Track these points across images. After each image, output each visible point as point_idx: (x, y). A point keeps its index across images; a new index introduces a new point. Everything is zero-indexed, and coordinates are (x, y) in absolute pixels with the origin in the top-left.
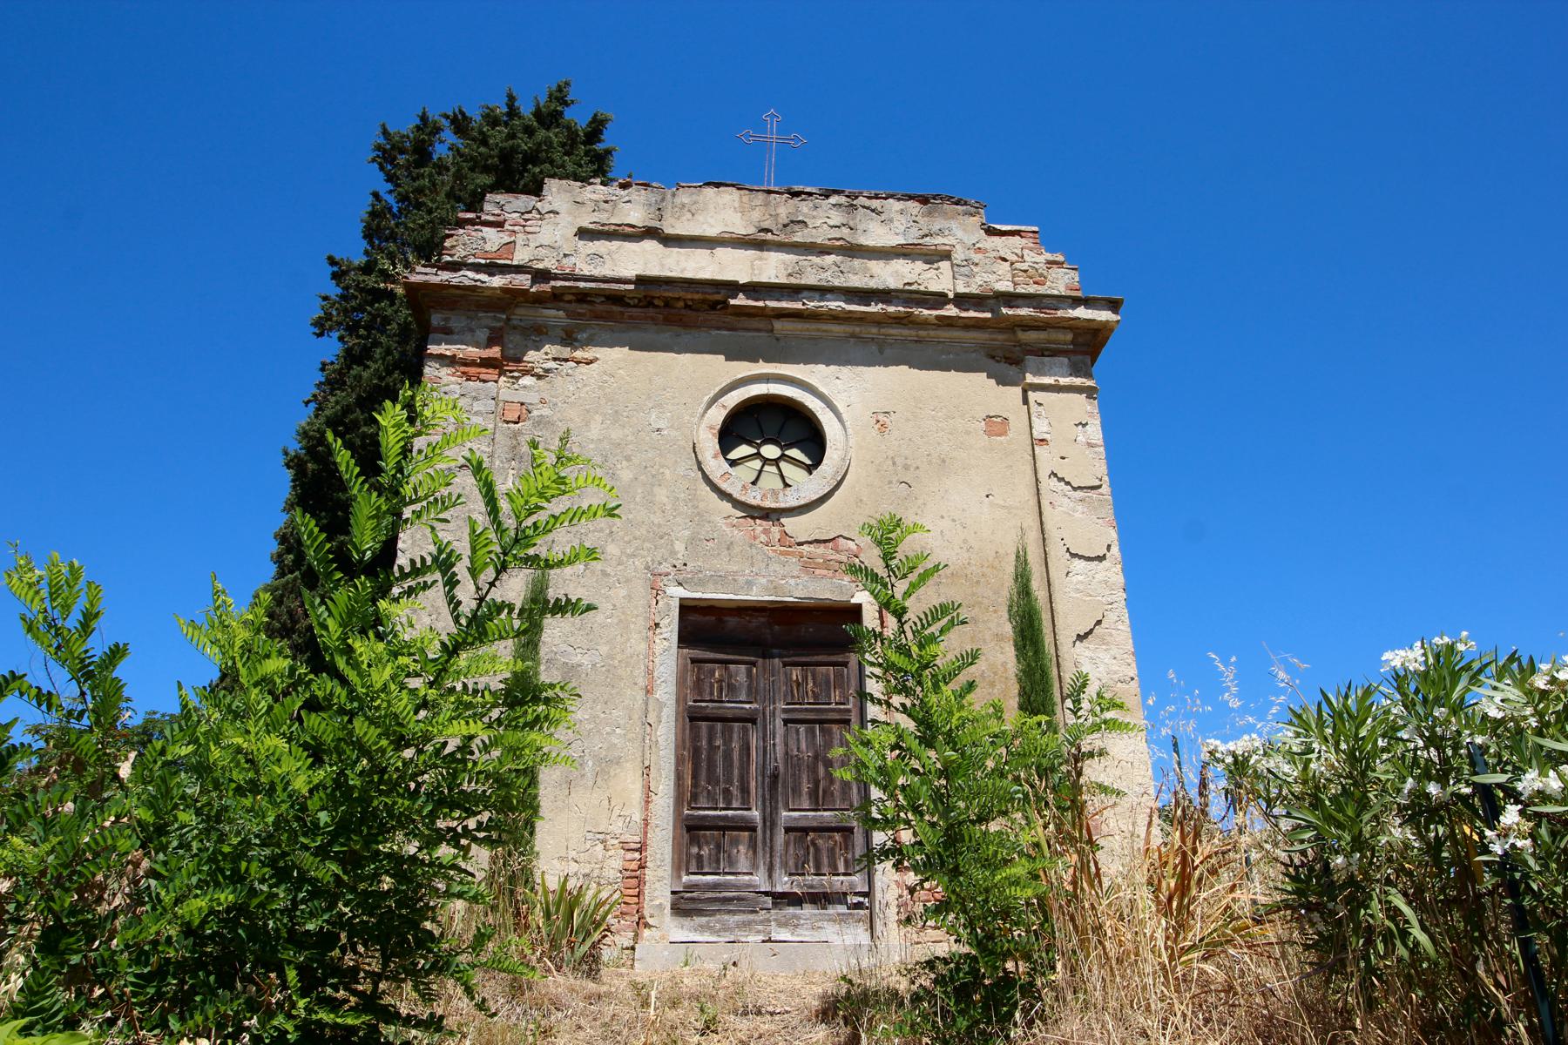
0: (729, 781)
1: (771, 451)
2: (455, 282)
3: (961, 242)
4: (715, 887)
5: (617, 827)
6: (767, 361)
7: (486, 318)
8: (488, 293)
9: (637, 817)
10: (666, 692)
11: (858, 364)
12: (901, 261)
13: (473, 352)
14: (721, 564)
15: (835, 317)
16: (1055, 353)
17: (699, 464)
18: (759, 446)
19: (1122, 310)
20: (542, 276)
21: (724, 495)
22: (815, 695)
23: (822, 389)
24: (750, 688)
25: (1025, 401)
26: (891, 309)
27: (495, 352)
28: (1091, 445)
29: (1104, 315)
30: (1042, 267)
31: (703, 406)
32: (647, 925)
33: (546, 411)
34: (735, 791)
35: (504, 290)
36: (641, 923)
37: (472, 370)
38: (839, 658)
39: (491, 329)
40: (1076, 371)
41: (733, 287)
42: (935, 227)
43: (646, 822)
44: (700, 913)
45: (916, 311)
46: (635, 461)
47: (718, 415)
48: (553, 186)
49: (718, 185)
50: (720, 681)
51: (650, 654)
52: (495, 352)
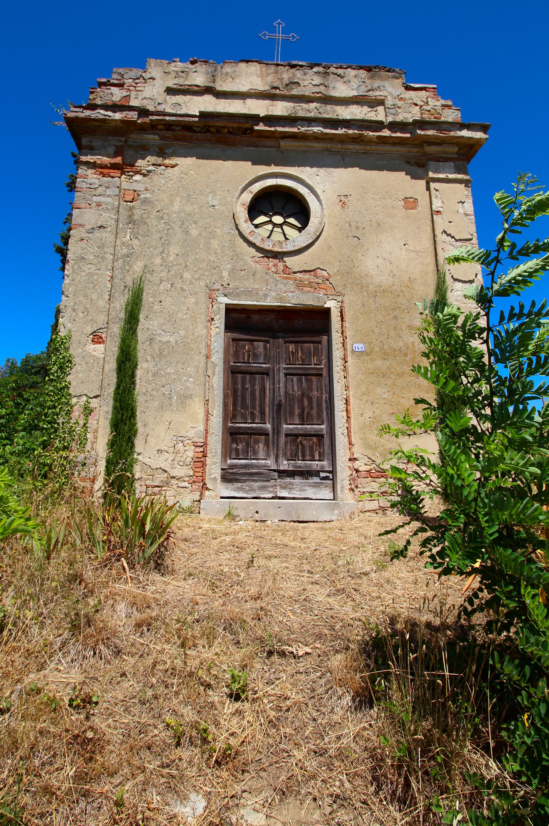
0: (254, 407)
1: (278, 219)
2: (93, 116)
3: (391, 94)
4: (246, 466)
5: (191, 433)
6: (276, 165)
7: (114, 141)
8: (113, 124)
9: (202, 428)
10: (218, 358)
11: (329, 167)
12: (355, 106)
13: (106, 160)
14: (250, 284)
15: (317, 138)
16: (446, 160)
17: (236, 225)
18: (271, 217)
19: (489, 131)
20: (143, 112)
21: (251, 244)
22: (303, 360)
23: (308, 181)
24: (265, 355)
25: (428, 188)
26: (351, 132)
27: (119, 160)
28: (466, 215)
29: (479, 135)
30: (439, 108)
31: (239, 191)
32: (207, 489)
33: (148, 195)
34: (257, 413)
35: (123, 121)
36: (204, 487)
37: (106, 171)
38: (317, 339)
39: (116, 146)
40: (458, 171)
41: (256, 119)
42: (376, 85)
43: (207, 431)
44: (237, 481)
45: (365, 133)
46: (200, 224)
47: (247, 197)
48: (152, 62)
49: (247, 62)
50: (249, 351)
51: (209, 335)
52: (119, 160)
